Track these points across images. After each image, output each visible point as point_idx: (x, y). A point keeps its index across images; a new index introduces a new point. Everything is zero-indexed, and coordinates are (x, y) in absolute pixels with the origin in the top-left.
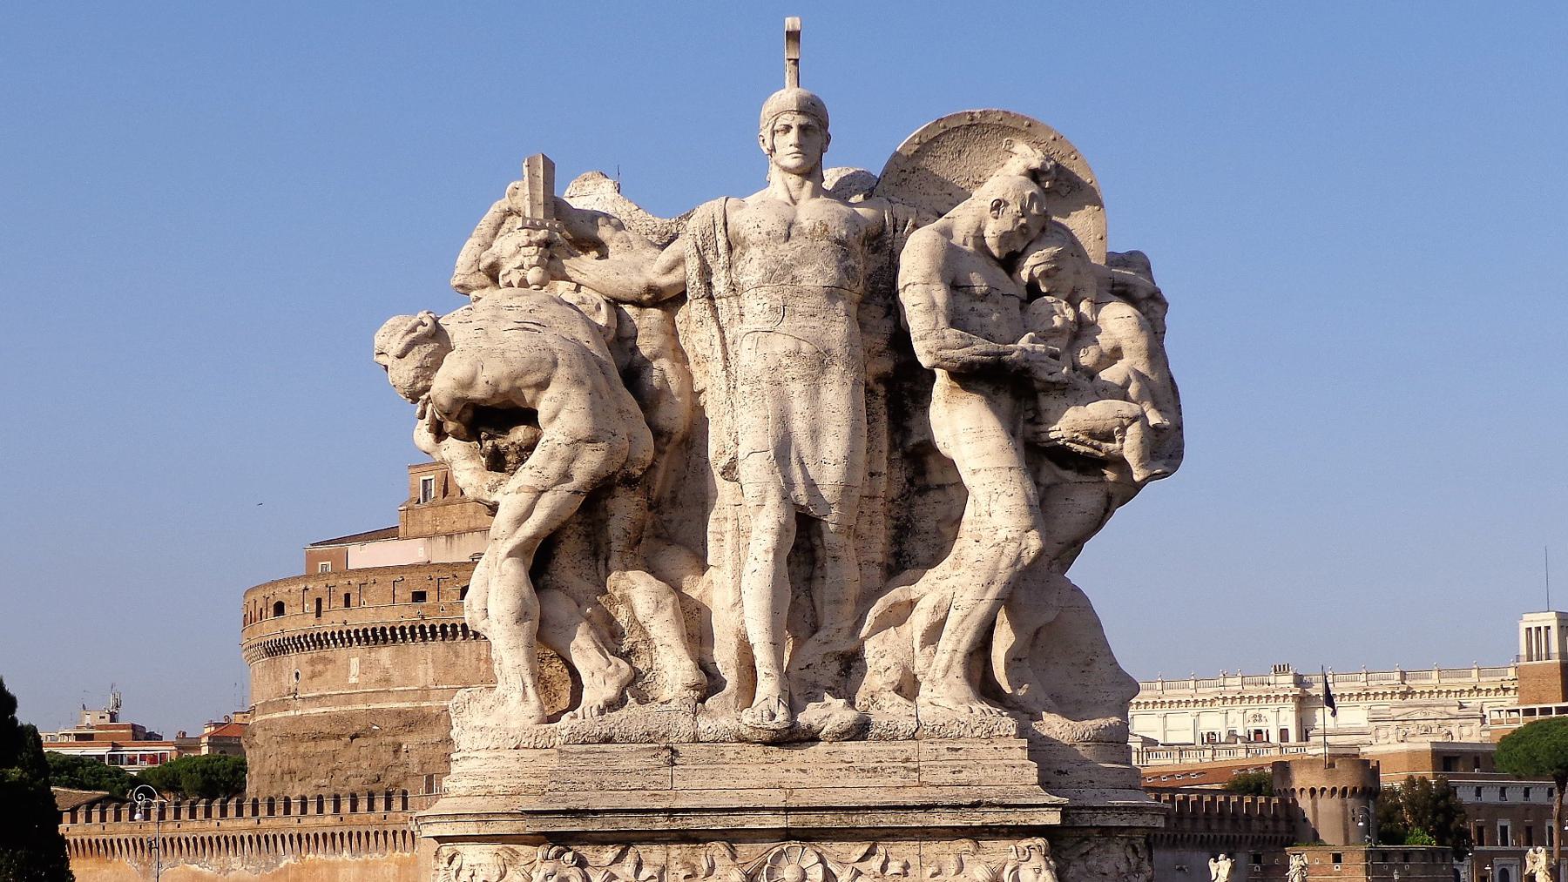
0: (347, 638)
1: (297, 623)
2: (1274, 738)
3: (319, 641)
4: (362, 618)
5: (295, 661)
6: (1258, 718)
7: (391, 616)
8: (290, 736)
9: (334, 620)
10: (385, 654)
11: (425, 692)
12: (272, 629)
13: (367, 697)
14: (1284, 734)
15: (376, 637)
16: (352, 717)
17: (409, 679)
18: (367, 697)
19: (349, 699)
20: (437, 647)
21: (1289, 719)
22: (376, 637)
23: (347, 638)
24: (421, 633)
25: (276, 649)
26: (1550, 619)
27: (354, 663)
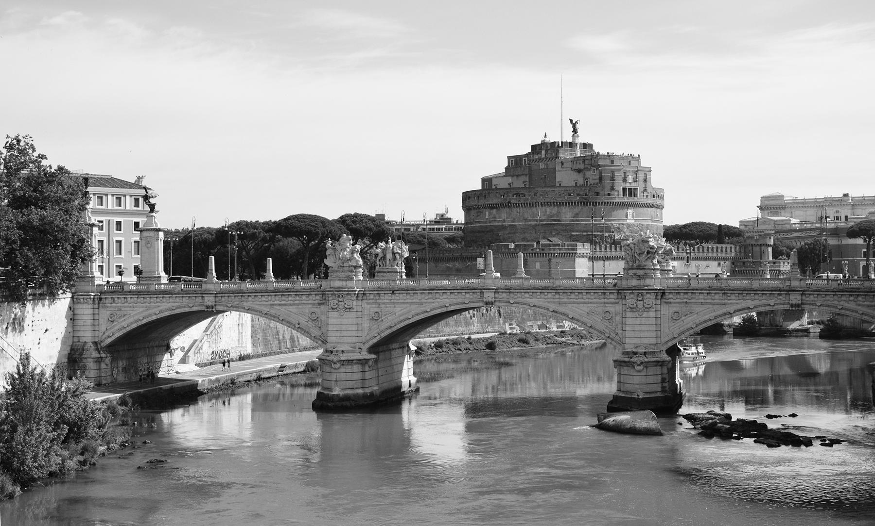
0: (486, 207)
1: (473, 202)
2: (843, 220)
6: (837, 212)
7: (495, 201)
9: (482, 202)
10: (494, 211)
11: (504, 221)
13: (490, 222)
14: (846, 217)
16: (486, 227)
17: (500, 217)
18: (490, 222)
19: (486, 222)
20: (507, 210)
22: (492, 207)
23: (486, 207)
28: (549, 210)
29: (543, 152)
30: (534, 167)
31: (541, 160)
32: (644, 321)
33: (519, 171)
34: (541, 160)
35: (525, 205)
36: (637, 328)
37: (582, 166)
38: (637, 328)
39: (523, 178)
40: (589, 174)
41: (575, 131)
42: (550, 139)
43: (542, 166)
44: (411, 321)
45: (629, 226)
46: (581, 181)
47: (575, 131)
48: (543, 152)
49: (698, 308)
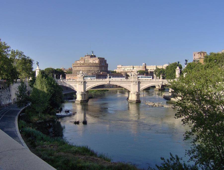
0: (77, 66)
3: (76, 66)
4: (78, 66)
5: (75, 67)
7: (79, 65)
8: (75, 71)
9: (77, 65)
10: (79, 67)
12: (73, 66)
14: (132, 69)
15: (79, 66)
20: (81, 67)
21: (132, 68)
22: (79, 66)
23: (77, 66)
24: (81, 66)
25: (74, 67)
26: (144, 64)
27: (77, 68)
28: (89, 67)
29: (87, 57)
30: (85, 59)
31: (87, 58)
32: (136, 87)
33: (82, 60)
34: (87, 58)
35: (85, 66)
36: (135, 88)
37: (95, 59)
38: (135, 88)
39: (83, 61)
40: (96, 61)
41: (93, 53)
42: (89, 54)
43: (87, 59)
44: (94, 87)
45: (103, 70)
46: (94, 62)
47: (93, 53)
48: (87, 57)
49: (145, 84)
